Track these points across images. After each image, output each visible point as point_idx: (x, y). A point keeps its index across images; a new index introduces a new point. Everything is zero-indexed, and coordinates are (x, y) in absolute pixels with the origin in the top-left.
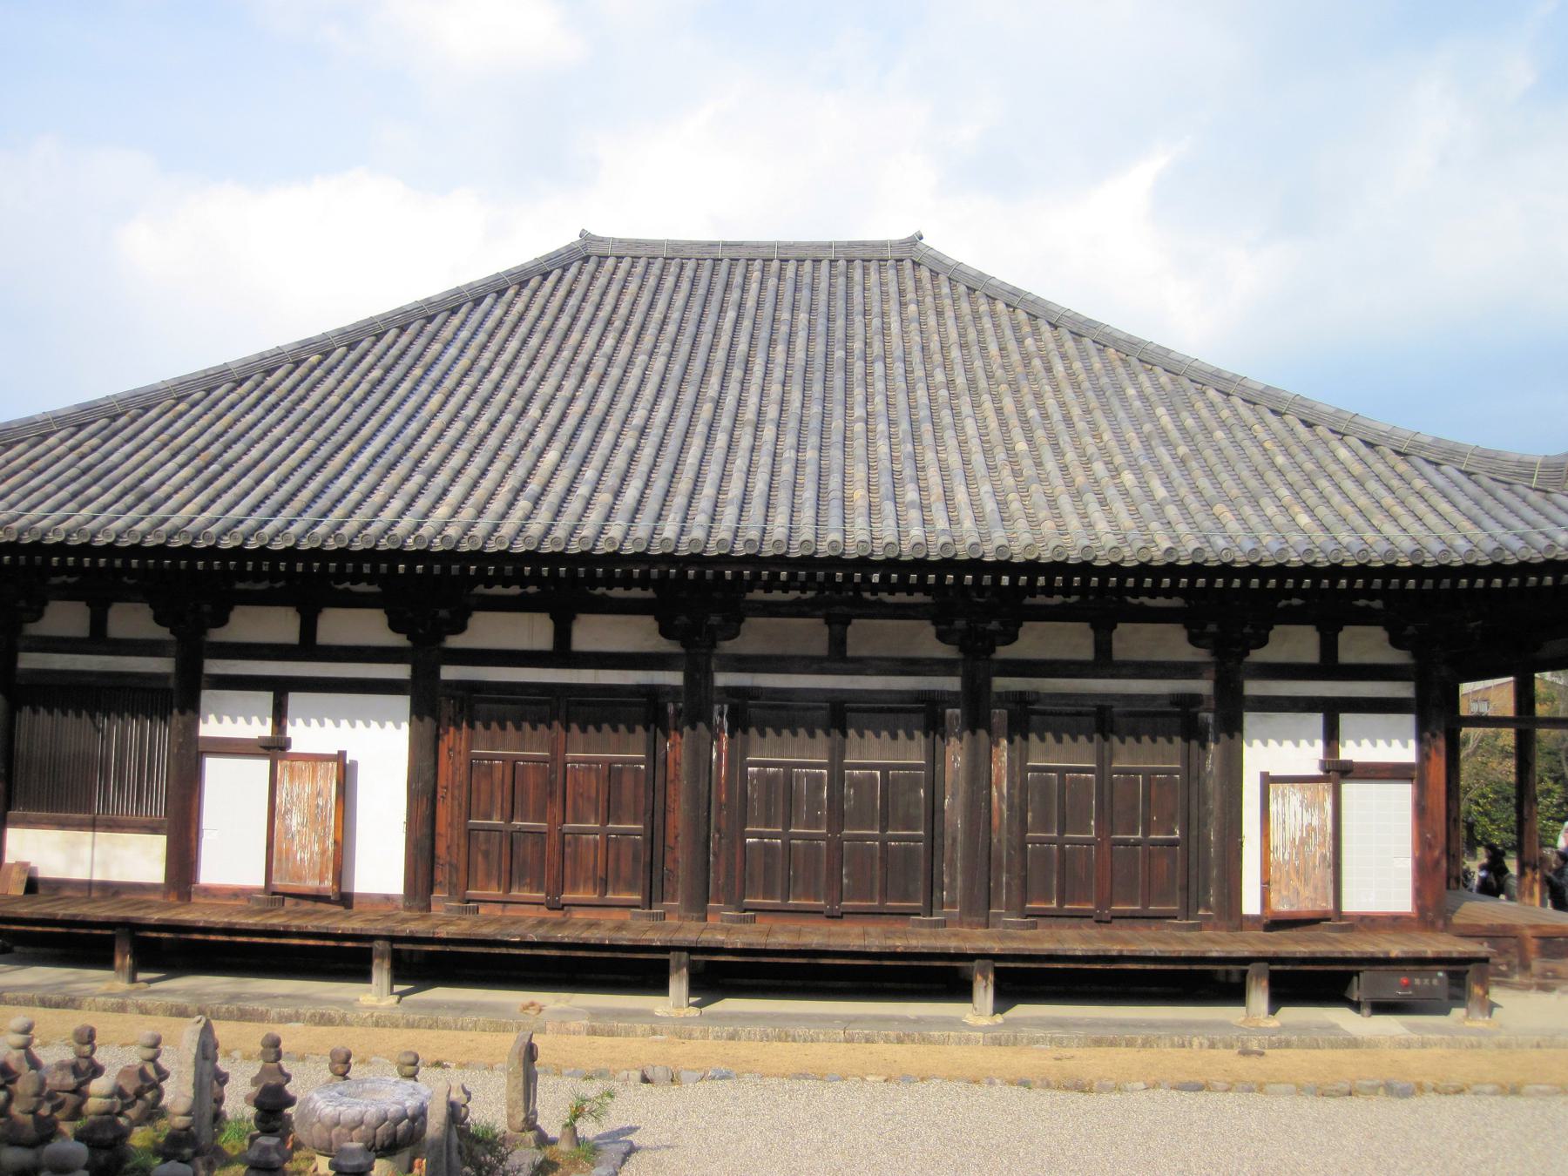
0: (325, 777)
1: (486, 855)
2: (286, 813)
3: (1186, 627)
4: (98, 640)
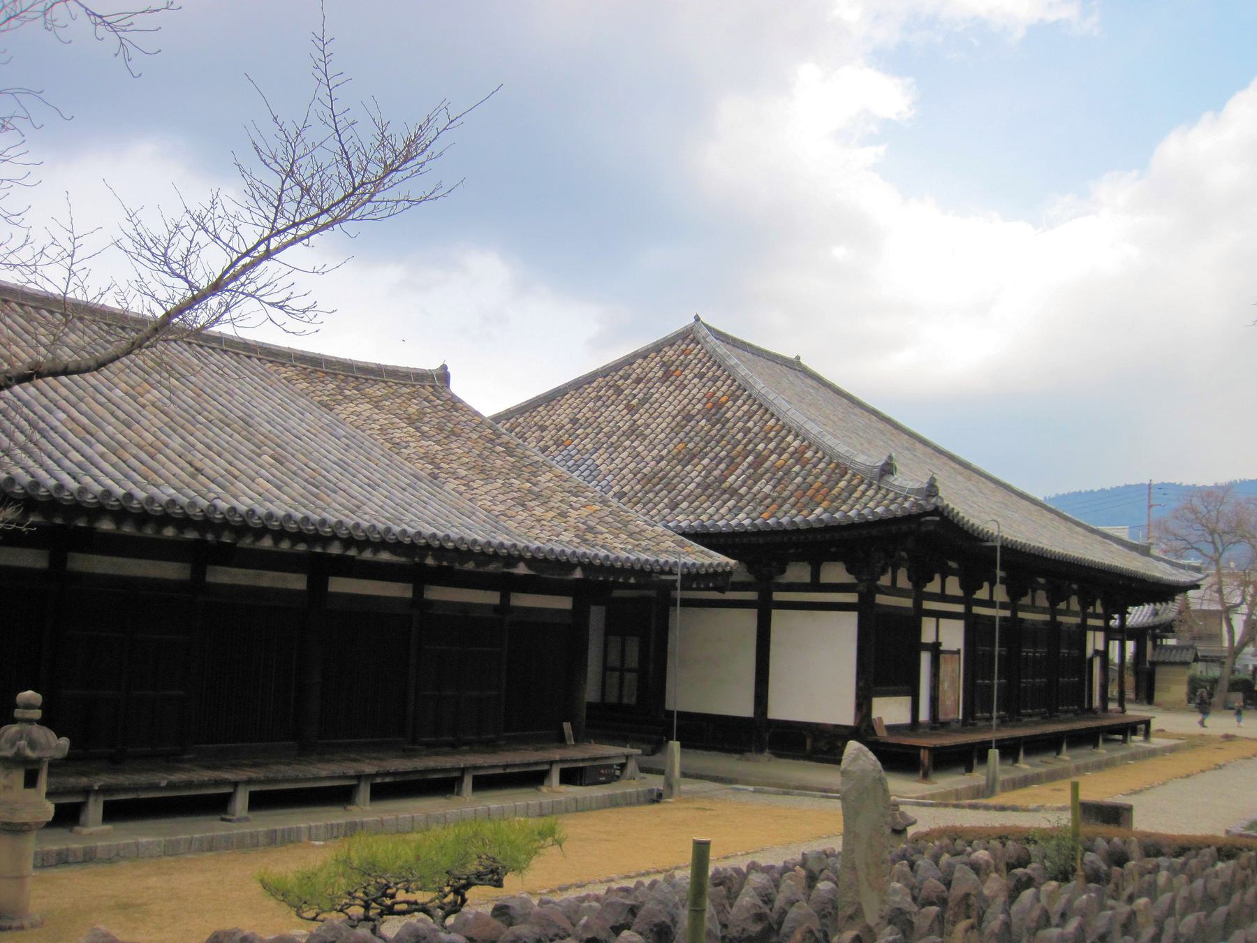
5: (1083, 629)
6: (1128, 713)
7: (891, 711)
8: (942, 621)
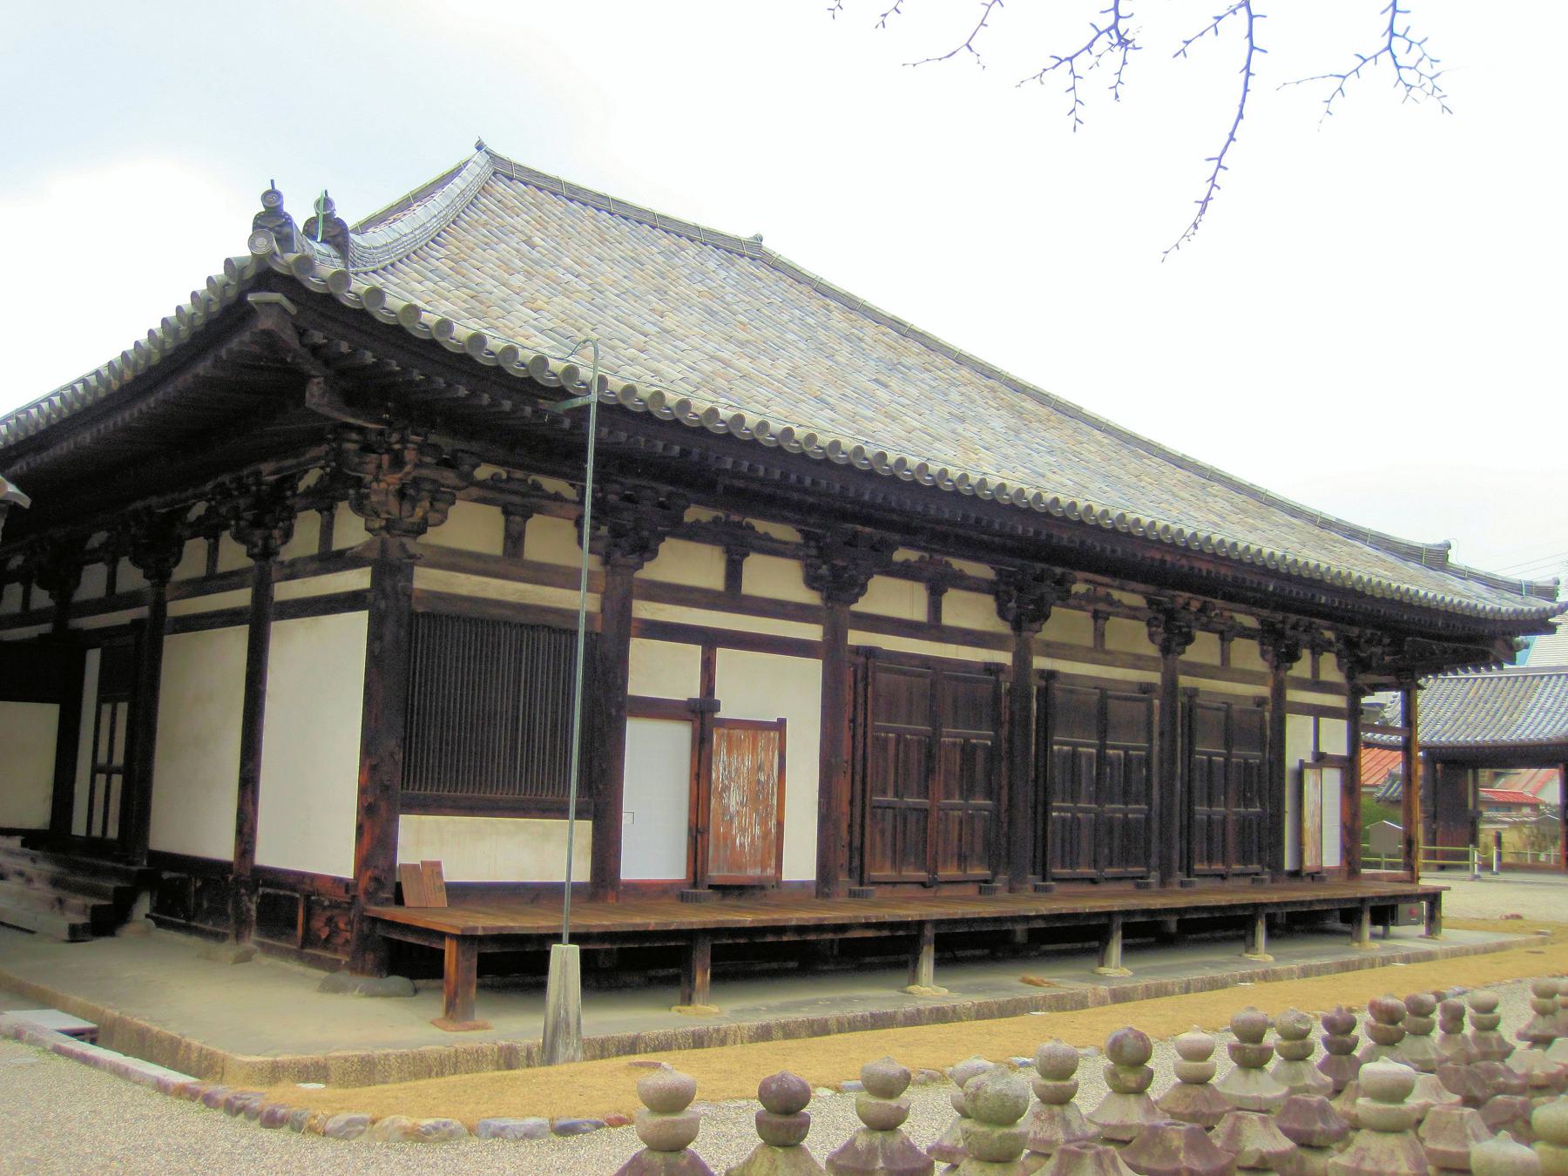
0: (766, 749)
1: (883, 832)
2: (723, 790)
3: (1262, 644)
4: (512, 558)
5: (1280, 708)
6: (1422, 882)
7: (475, 852)
8: (722, 654)
